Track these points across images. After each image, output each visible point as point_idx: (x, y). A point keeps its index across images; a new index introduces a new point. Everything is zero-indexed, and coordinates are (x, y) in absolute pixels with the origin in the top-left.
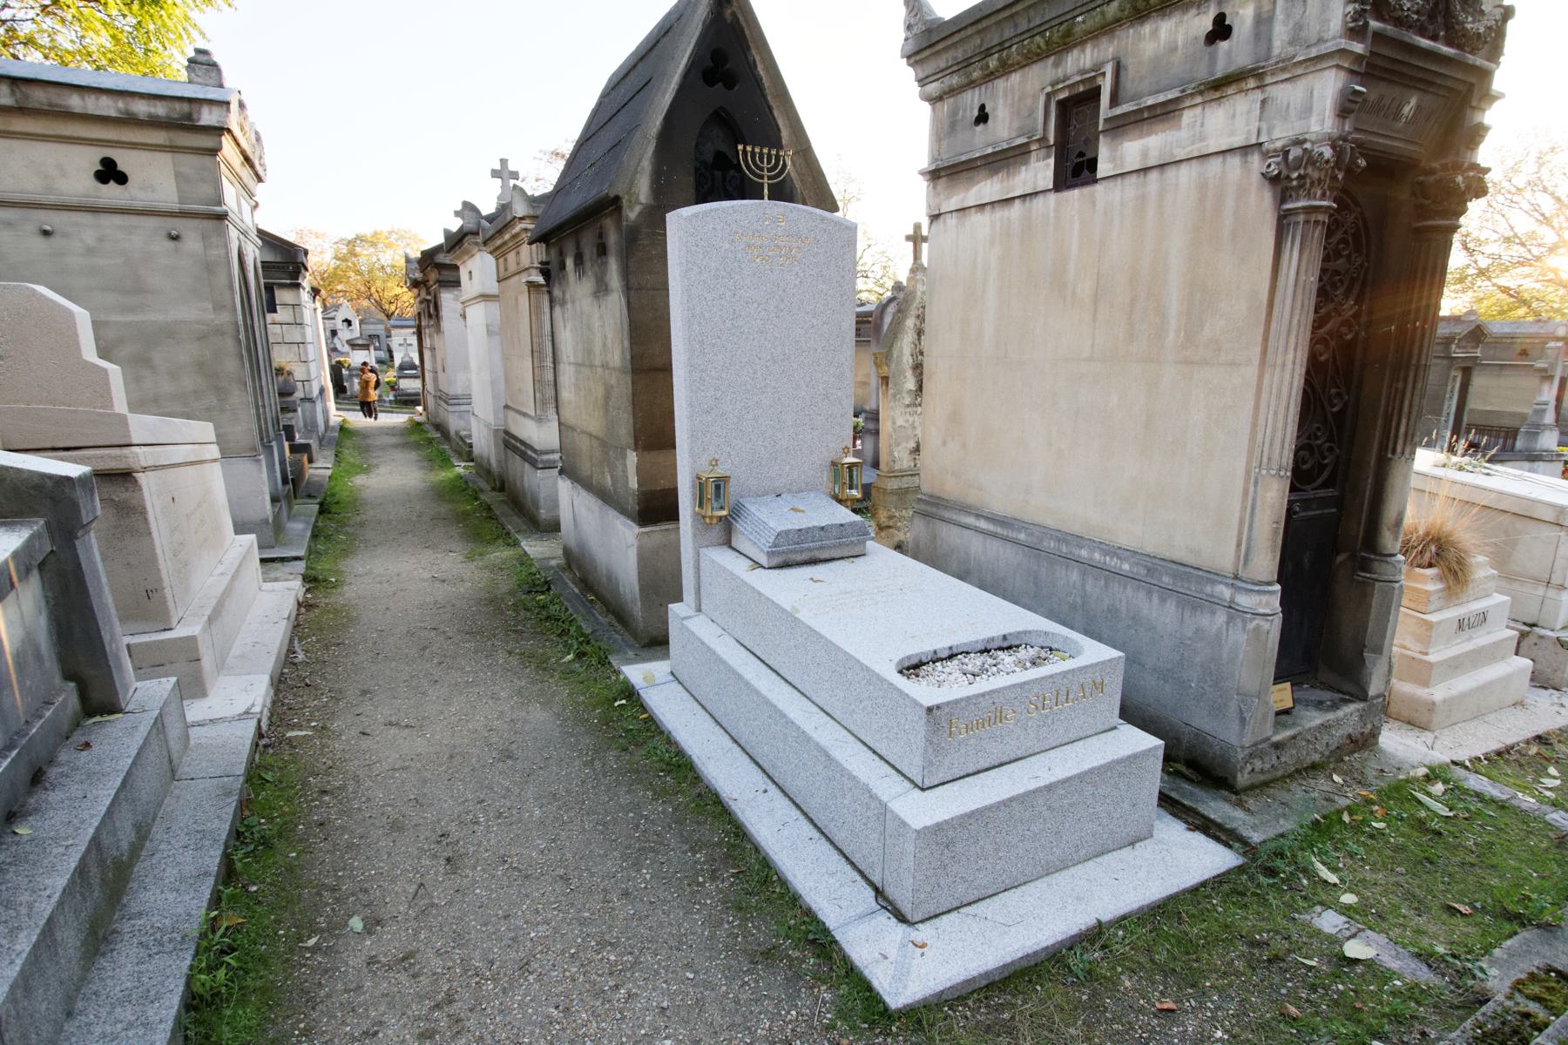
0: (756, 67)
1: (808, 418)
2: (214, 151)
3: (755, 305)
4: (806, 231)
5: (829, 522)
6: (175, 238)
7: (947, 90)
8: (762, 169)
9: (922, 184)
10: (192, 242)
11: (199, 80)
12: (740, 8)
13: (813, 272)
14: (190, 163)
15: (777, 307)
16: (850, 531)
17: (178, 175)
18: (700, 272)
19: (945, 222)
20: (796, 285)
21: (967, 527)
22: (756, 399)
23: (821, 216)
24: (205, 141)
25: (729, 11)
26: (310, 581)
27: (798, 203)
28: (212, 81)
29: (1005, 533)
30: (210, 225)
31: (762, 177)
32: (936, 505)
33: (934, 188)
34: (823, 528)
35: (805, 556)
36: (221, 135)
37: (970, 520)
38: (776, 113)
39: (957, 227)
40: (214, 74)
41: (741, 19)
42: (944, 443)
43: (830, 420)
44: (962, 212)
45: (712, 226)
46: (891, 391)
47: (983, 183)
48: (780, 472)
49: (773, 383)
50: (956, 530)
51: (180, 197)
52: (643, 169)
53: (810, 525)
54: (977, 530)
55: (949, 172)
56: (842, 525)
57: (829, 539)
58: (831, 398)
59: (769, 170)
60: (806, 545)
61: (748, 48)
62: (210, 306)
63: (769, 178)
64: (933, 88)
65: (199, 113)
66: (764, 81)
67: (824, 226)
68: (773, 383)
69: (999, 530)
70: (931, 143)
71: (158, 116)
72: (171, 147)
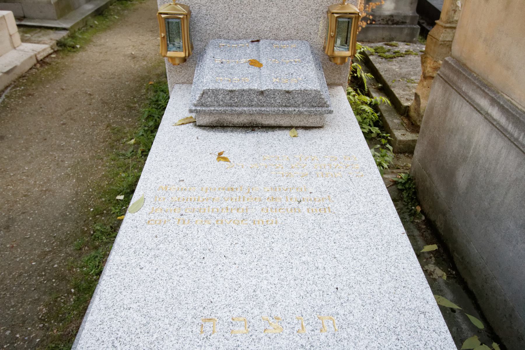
5: (271, 87)
16: (299, 100)
21: (478, 109)
26: (61, 46)
29: (516, 135)
32: (457, 73)
34: (262, 93)
35: (243, 120)
37: (484, 103)
48: (266, 14)
50: (467, 109)
53: (246, 88)
56: (288, 92)
57: (271, 105)
69: (510, 127)
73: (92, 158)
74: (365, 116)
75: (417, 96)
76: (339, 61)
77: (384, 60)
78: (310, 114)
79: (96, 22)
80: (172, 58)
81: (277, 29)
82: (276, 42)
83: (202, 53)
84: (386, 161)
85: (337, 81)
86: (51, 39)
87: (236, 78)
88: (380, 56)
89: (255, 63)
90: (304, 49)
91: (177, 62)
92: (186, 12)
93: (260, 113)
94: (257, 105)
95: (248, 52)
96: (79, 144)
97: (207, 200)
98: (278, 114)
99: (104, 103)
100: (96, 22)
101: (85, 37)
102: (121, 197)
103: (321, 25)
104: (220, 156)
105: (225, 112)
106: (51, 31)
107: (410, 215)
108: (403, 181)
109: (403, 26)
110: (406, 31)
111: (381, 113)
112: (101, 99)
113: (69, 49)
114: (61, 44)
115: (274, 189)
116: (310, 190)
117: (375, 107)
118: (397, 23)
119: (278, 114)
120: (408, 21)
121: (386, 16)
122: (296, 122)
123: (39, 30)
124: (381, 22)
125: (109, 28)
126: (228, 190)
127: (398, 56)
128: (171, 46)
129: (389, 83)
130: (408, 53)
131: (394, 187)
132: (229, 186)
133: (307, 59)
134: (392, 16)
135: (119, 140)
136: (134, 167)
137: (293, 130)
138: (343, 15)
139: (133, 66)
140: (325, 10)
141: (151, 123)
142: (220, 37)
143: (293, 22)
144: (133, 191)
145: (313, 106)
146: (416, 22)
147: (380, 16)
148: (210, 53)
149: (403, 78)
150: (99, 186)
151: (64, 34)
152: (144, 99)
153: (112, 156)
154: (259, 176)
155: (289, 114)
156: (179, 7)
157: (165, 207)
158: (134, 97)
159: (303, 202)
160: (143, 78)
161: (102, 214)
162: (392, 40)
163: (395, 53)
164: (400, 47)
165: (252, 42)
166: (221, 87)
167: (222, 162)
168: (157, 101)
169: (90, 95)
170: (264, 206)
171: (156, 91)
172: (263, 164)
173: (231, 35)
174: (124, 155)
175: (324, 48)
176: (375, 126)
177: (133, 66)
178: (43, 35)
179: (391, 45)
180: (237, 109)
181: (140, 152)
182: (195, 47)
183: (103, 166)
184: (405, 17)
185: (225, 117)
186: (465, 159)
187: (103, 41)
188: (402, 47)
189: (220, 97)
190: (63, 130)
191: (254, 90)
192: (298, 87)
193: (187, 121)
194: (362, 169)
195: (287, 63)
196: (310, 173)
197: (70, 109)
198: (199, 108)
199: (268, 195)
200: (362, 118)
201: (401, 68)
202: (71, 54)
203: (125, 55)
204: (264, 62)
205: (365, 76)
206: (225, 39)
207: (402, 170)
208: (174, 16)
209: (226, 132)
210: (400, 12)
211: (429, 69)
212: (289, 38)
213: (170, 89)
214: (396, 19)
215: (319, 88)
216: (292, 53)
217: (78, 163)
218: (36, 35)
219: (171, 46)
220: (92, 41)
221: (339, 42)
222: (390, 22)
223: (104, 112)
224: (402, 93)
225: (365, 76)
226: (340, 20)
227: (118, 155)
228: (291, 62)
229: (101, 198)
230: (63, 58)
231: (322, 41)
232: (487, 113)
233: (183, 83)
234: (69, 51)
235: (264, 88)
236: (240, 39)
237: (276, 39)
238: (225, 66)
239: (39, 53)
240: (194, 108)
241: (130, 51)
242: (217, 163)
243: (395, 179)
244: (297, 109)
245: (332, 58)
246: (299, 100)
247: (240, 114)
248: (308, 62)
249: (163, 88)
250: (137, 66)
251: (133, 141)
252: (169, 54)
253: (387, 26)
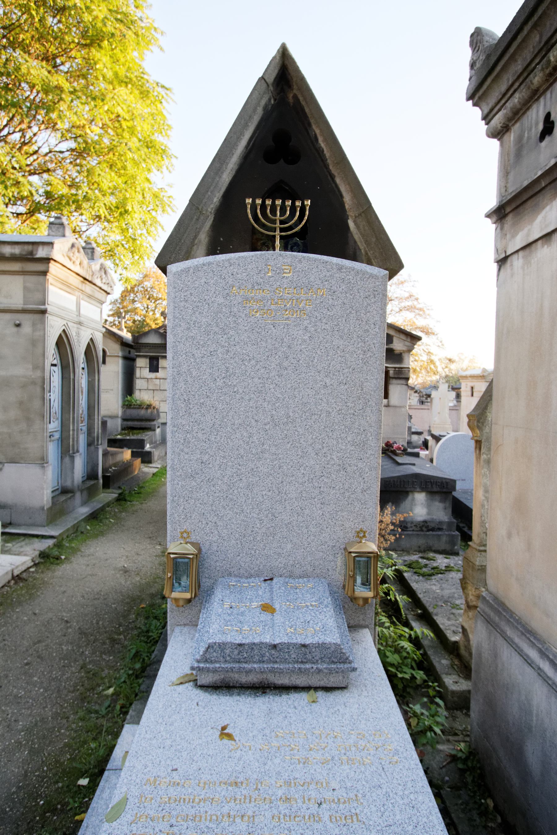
0: (317, 140)
1: (317, 491)
2: (45, 273)
3: (253, 362)
4: (319, 282)
5: (285, 640)
6: (18, 325)
7: (510, 114)
8: (274, 222)
9: (490, 227)
10: (27, 329)
11: (53, 234)
12: (299, 89)
13: (327, 327)
14: (32, 280)
15: (280, 364)
16: (317, 654)
17: (26, 289)
18: (188, 329)
19: (512, 265)
20: (305, 341)
22: (252, 465)
23: (337, 264)
24: (40, 267)
25: (291, 96)
27: (362, 262)
28: (60, 234)
30: (37, 316)
31: (274, 230)
33: (502, 229)
34: (275, 646)
35: (252, 678)
36: (49, 263)
38: (338, 180)
39: (523, 268)
40: (61, 230)
41: (301, 99)
42: (509, 535)
43: (347, 494)
44: (527, 251)
45: (204, 280)
46: (484, 457)
47: (548, 208)
48: (279, 550)
49: (273, 449)
50: (516, 660)
51: (24, 301)
52: (200, 241)
53: (257, 641)
54: (540, 672)
55: (514, 206)
56: (304, 646)
57: (285, 661)
58: (349, 469)
59: (282, 222)
60: (248, 666)
61: (310, 125)
62: (31, 367)
63: (282, 230)
64: (498, 120)
65: (37, 250)
66: (325, 152)
67: (343, 275)
68: (273, 449)
70: (499, 180)
71: (15, 255)
72: (22, 272)
73: (56, 716)
74: (405, 654)
75: (464, 630)
76: (361, 602)
77: (421, 578)
78: (331, 672)
79: (88, 527)
80: (176, 600)
81: (292, 565)
82: (291, 580)
83: (210, 592)
84: (438, 723)
85: (362, 622)
86: (35, 550)
87: (246, 628)
88: (415, 573)
89: (267, 608)
90: (321, 589)
91: (181, 603)
92: (195, 552)
93: (272, 671)
94: (269, 661)
95: (260, 593)
96: (42, 694)
97: (205, 800)
98: (293, 672)
99: (82, 632)
100: (88, 527)
101: (73, 545)
102: (84, 782)
103: (340, 561)
104: (225, 733)
105: (232, 669)
106: (36, 540)
107: (481, 814)
108: (464, 756)
109: (440, 533)
110: (444, 539)
111: (425, 650)
112: (79, 628)
113: (52, 560)
114: (44, 555)
115: (288, 783)
116: (334, 785)
117: (416, 642)
118: (433, 530)
119: (293, 672)
120: (445, 527)
121: (420, 522)
122: (315, 681)
123: (23, 538)
124: (414, 528)
125: (102, 534)
126: (230, 784)
127: (438, 574)
128: (176, 585)
129: (431, 609)
130: (448, 569)
131: (452, 765)
132: (232, 779)
133: (325, 602)
134: (425, 522)
135: (93, 689)
136: (108, 732)
137: (312, 691)
138: (361, 554)
139: (123, 582)
140: (342, 547)
141: (138, 666)
142: (230, 575)
143: (309, 559)
144: (101, 772)
145: (333, 662)
146: (454, 528)
147: (412, 523)
148: (218, 594)
149: (446, 602)
150: (57, 761)
151: (50, 542)
152: (132, 629)
153: (81, 714)
154: (269, 763)
155: (305, 672)
156: (189, 546)
157: (152, 813)
158: (120, 625)
159: (324, 806)
160: (133, 600)
161: (54, 811)
162: (430, 549)
163: (433, 568)
164: (439, 561)
165: (265, 580)
166: (229, 639)
167: (226, 741)
168: (148, 631)
169: (67, 622)
170: (276, 813)
171: (147, 618)
172: (275, 744)
173: (242, 571)
174: (97, 712)
175: (344, 586)
176: (419, 669)
177: (123, 582)
178: (26, 544)
179: (428, 559)
180: (246, 666)
181: (118, 707)
182: (202, 584)
183: (67, 729)
184: (441, 523)
185: (232, 675)
186: (530, 729)
187: (92, 550)
188: (441, 561)
189: (227, 652)
190: (25, 673)
191: (266, 643)
192: (315, 640)
193: (186, 679)
194: (396, 752)
195: (303, 607)
196: (333, 758)
197: (39, 642)
198: (202, 665)
199: (280, 793)
200: (401, 657)
201: (442, 589)
202: (53, 567)
203: (115, 569)
204: (277, 606)
205: (402, 599)
206: (236, 576)
207: (461, 737)
208: (183, 556)
209: (231, 695)
210: (435, 517)
211: (471, 597)
212: (305, 575)
213: (169, 632)
214: (432, 525)
215: (338, 641)
216: (308, 595)
217: (36, 724)
218: (19, 544)
219: (176, 585)
220: (80, 550)
221: (359, 580)
222: (424, 529)
223: (80, 647)
224: (448, 623)
225: (402, 599)
226: (357, 559)
227: (90, 712)
228: (307, 606)
229: (57, 782)
230: (42, 572)
231: (341, 578)
232: (539, 668)
233: (185, 625)
234: (52, 563)
235: (277, 641)
236: (251, 576)
237: (290, 576)
238: (235, 611)
239: (17, 567)
240: (196, 665)
241: (123, 563)
242: (219, 742)
243: (453, 752)
244: (315, 667)
245: (353, 599)
246: (317, 654)
247: (249, 672)
248: (326, 606)
249: (157, 612)
250: (128, 583)
251: (111, 690)
252: (174, 595)
253: (422, 533)
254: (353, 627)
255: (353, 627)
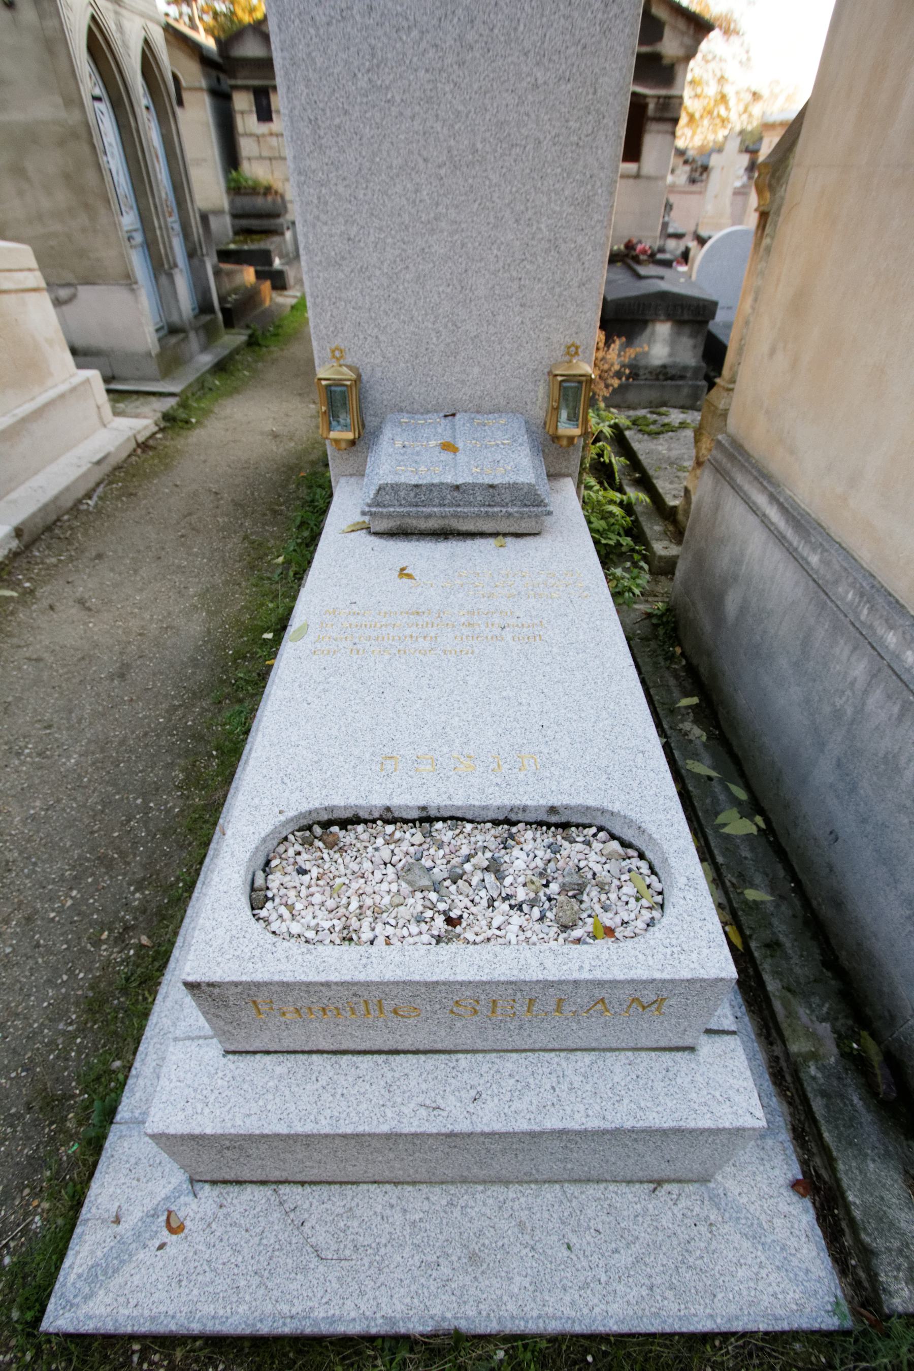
1: (515, 285)
3: (415, 33)
5: (470, 480)
16: (507, 497)
21: (754, 509)
29: (795, 544)
32: (732, 457)
34: (457, 488)
35: (433, 524)
37: (761, 500)
42: (773, 352)
43: (557, 290)
46: (766, 241)
48: (464, 376)
53: (436, 481)
54: (764, 520)
56: (492, 486)
57: (470, 504)
58: (563, 247)
69: (789, 533)
73: (226, 583)
74: (612, 520)
75: (687, 491)
76: (564, 442)
77: (646, 436)
78: (522, 516)
79: (217, 383)
80: (337, 441)
81: (480, 397)
82: (478, 416)
83: (376, 434)
84: (638, 586)
85: (564, 471)
86: (155, 411)
87: (423, 468)
88: (640, 431)
89: (449, 447)
90: (516, 425)
91: (343, 445)
92: (354, 376)
93: (456, 515)
94: (451, 505)
95: (440, 430)
96: (207, 564)
97: (386, 626)
98: (478, 516)
99: (236, 504)
100: (217, 383)
101: (203, 405)
102: (269, 636)
103: (542, 391)
104: (403, 573)
105: (409, 514)
106: (153, 399)
107: (666, 659)
108: (659, 613)
109: (680, 383)
110: (685, 391)
111: (637, 519)
112: (233, 500)
113: (180, 424)
114: (168, 417)
115: (471, 613)
116: (518, 614)
117: (628, 508)
118: (672, 378)
119: (478, 516)
120: (689, 375)
121: (658, 367)
122: (503, 527)
123: (135, 397)
124: (648, 376)
125: (236, 391)
126: (412, 614)
127: (668, 431)
128: (334, 423)
129: (651, 472)
130: (683, 425)
131: (647, 621)
132: (414, 610)
133: (520, 441)
134: (664, 367)
135: (261, 558)
136: (285, 596)
137: (500, 537)
138: (569, 378)
139: (274, 448)
140: (546, 370)
141: (306, 534)
142: (401, 410)
143: (502, 388)
144: (284, 628)
145: (526, 505)
146: (701, 376)
147: (646, 368)
148: (388, 432)
149: (671, 464)
150: (237, 621)
151: (172, 402)
152: (294, 499)
153: (253, 581)
154: (452, 597)
155: (493, 516)
156: (345, 369)
157: (334, 635)
158: (280, 496)
159: (507, 629)
160: (291, 468)
161: (244, 658)
162: (664, 404)
163: (664, 425)
164: (673, 416)
165: (446, 416)
166: (403, 479)
167: (405, 580)
168: (312, 501)
169: (216, 493)
170: (458, 634)
171: (310, 487)
172: (458, 582)
173: (416, 406)
174: (269, 579)
175: (545, 424)
176: (627, 535)
177: (274, 448)
178: (142, 404)
179: (659, 414)
180: (424, 509)
181: (291, 574)
182: (367, 424)
183: (241, 594)
184: (685, 368)
185: (409, 521)
186: (735, 578)
187: (228, 411)
188: (675, 416)
189: (402, 494)
190: (183, 545)
191: (447, 484)
192: (506, 480)
193: (358, 527)
194: (587, 588)
195: (492, 446)
196: (519, 593)
197: (190, 514)
198: (373, 509)
199: (463, 620)
200: (608, 524)
201: (669, 449)
202: (184, 433)
203: (262, 433)
204: (460, 445)
205: (618, 462)
206: (408, 412)
207: (660, 599)
208: (338, 383)
209: (410, 541)
210: (678, 360)
211: (704, 451)
212: (497, 410)
213: (333, 484)
214: (672, 372)
215: (533, 481)
216: (499, 433)
217: (208, 590)
218: (133, 405)
219: (334, 423)
220: (212, 412)
221: (564, 415)
222: (661, 377)
223: (238, 519)
224: (668, 486)
225: (618, 462)
226: (565, 384)
227: (262, 579)
228: (497, 445)
229: (242, 637)
230: (172, 439)
231: (542, 414)
232: (764, 515)
233: (351, 475)
234: (182, 428)
235: (460, 481)
236: (428, 412)
237: (478, 412)
238: (409, 451)
239: (139, 432)
240: (367, 509)
241: (270, 426)
242: (398, 581)
243: (649, 611)
244: (504, 510)
245: (556, 438)
246: (507, 497)
247: (429, 516)
248: (521, 445)
249: (321, 481)
250: (281, 450)
251: (281, 559)
252: (333, 435)
253: (657, 383)
254: (553, 476)
255: (553, 476)
